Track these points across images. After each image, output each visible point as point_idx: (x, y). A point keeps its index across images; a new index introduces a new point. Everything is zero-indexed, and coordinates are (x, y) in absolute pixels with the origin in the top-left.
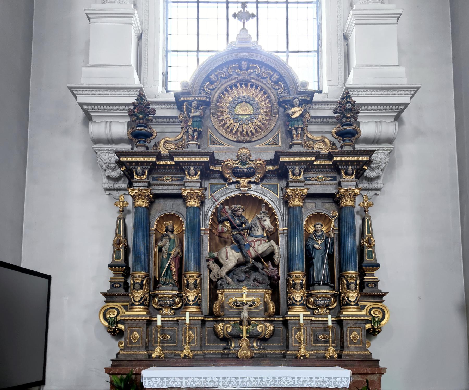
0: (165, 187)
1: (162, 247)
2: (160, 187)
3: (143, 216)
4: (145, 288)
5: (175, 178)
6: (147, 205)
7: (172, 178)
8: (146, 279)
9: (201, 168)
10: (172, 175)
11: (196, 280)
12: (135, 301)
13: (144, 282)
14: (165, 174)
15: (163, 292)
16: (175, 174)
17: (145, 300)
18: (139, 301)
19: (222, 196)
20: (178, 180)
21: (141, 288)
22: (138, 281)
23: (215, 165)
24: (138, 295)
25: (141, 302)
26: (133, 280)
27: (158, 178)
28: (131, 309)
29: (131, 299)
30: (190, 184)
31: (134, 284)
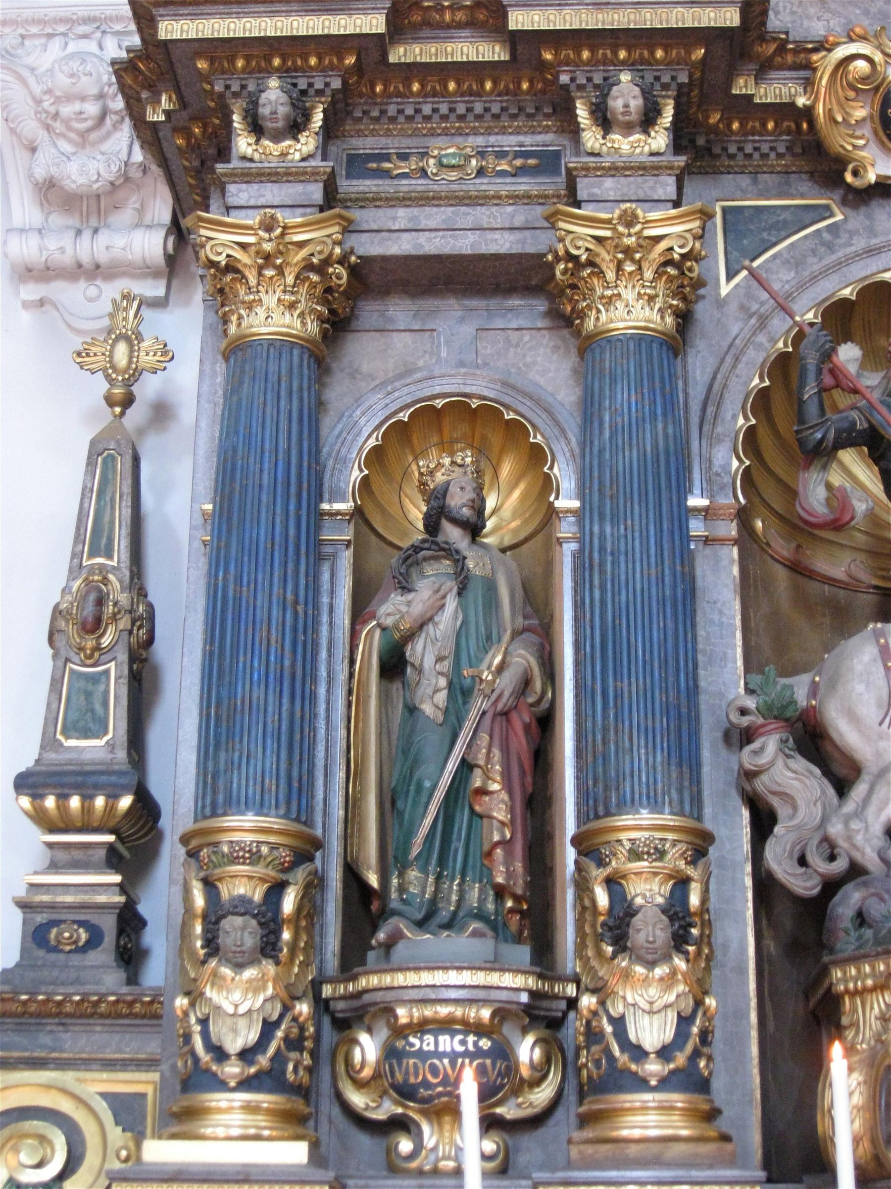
0: (435, 216)
1: (410, 636)
2: (402, 216)
3: (277, 405)
4: (293, 947)
5: (501, 155)
6: (313, 328)
7: (482, 154)
8: (300, 875)
9: (683, 78)
10: (480, 141)
11: (682, 883)
12: (220, 1054)
13: (289, 903)
14: (432, 134)
15: (426, 978)
16: (503, 131)
17: (294, 1043)
18: (247, 1055)
19: (814, 279)
20: (518, 172)
21: (268, 947)
22: (243, 885)
23: (764, 69)
24: (240, 1001)
25: (263, 1061)
26: (209, 885)
27: (387, 158)
28: (182, 1119)
29: (187, 1037)
30: (609, 186)
31: (214, 917)
